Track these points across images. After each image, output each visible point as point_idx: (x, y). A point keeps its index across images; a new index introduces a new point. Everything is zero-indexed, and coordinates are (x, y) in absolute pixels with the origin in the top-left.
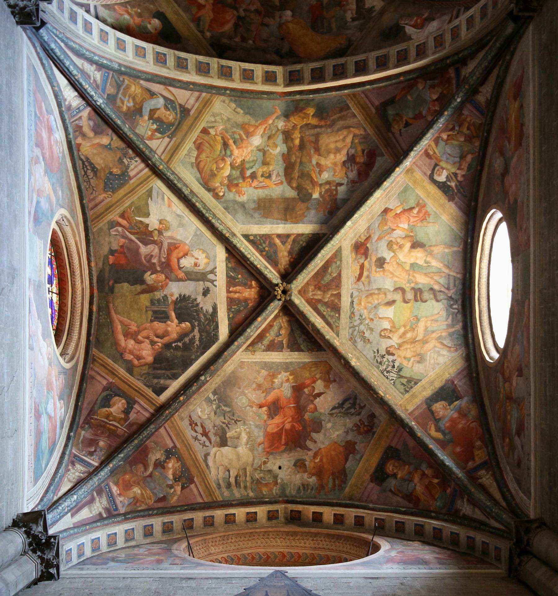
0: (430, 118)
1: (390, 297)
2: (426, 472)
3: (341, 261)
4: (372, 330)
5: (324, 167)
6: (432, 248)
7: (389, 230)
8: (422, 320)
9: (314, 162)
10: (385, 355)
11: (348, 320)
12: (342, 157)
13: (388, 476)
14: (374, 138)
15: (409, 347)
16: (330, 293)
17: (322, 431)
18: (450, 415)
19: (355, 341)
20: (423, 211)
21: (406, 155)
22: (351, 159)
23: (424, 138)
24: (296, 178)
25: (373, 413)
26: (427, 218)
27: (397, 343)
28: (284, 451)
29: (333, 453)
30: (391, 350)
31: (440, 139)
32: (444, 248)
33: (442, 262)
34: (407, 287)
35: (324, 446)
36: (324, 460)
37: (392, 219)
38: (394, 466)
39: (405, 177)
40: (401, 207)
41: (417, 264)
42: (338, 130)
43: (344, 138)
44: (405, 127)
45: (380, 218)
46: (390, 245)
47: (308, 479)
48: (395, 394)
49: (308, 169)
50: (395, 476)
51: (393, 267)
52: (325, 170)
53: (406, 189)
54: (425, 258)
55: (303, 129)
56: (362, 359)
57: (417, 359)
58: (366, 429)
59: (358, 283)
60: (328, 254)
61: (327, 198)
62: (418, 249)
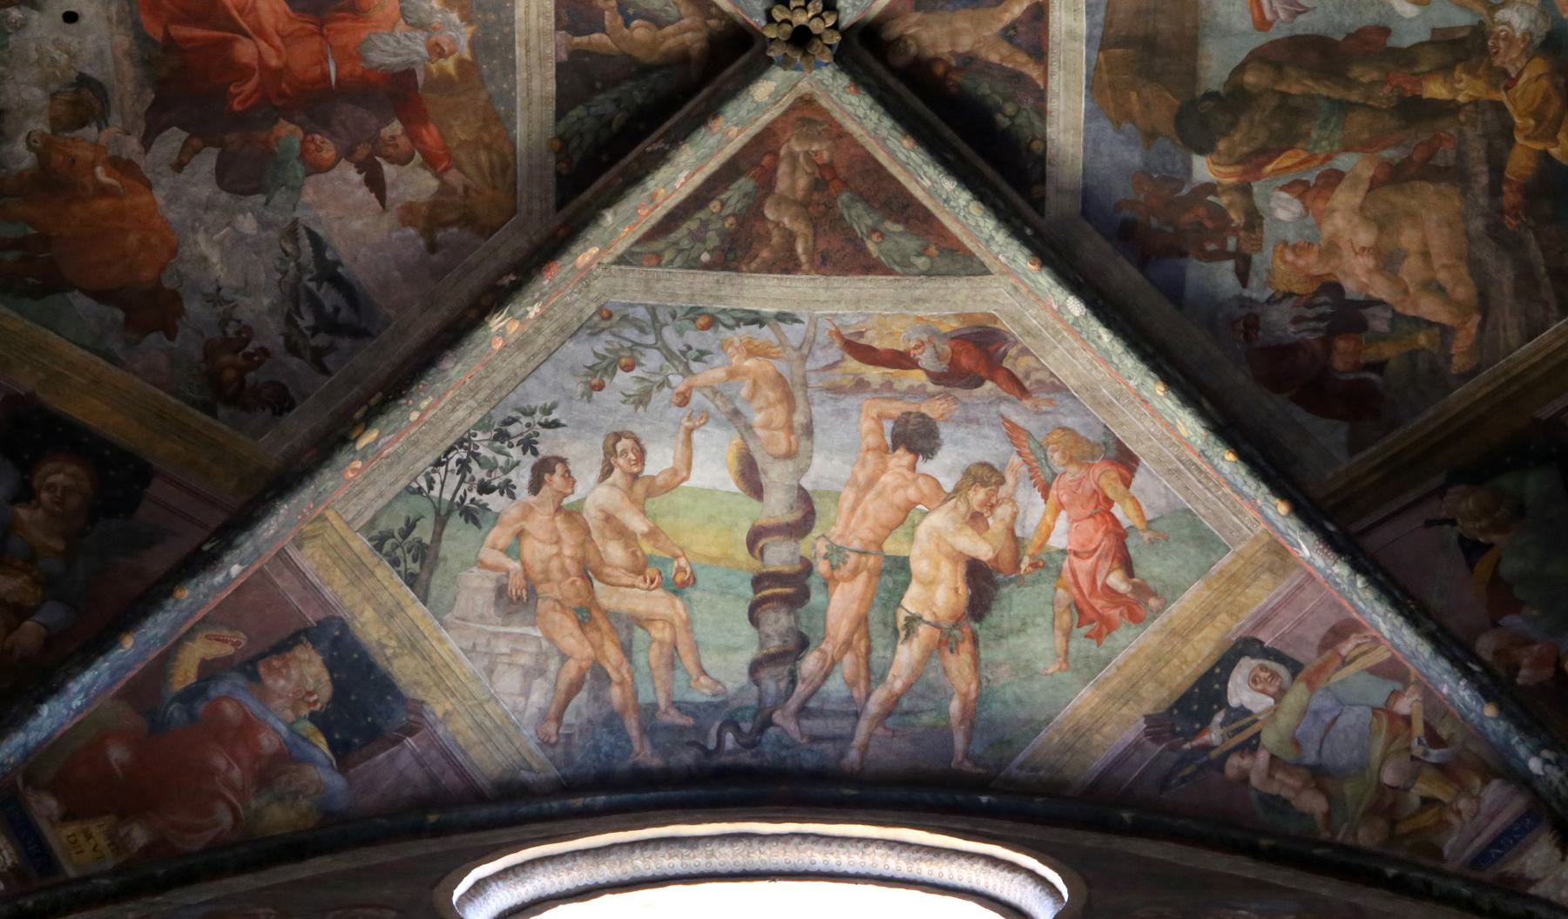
0: (1486, 645)
1: (775, 475)
2: (28, 623)
3: (929, 273)
4: (642, 399)
5: (1320, 204)
6: (966, 647)
7: (1045, 474)
8: (678, 603)
9: (1344, 162)
10: (535, 453)
11: (684, 302)
12: (1358, 276)
13: (26, 468)
14: (1431, 412)
15: (567, 551)
16: (799, 227)
17: (224, 197)
18: (271, 719)
19: (595, 333)
20: (1115, 613)
21: (1342, 544)
22: (1345, 314)
23: (1399, 621)
24: (1283, 87)
25: (290, 409)
26: (1086, 629)
27: (582, 501)
28: (141, 37)
29: (133, 239)
30: (557, 479)
31: (1398, 686)
32: (965, 695)
33: (908, 687)
34: (813, 546)
35: (160, 201)
36: (103, 205)
37: (1089, 485)
38: (65, 489)
39: (1257, 539)
40: (1137, 522)
41: (906, 585)
42: (1475, 266)
43: (1440, 289)
44: (1462, 540)
45: (1096, 436)
46: (984, 475)
47: (23, 136)
48: (370, 494)
49: (1314, 135)
50: (25, 494)
51: (897, 488)
52: (1306, 208)
53: (1206, 542)
54: (927, 617)
55: (1489, 116)
56: (520, 359)
57: (516, 585)
58: (230, 374)
59: (838, 344)
60: (957, 220)
61: (1187, 218)
62: (964, 592)
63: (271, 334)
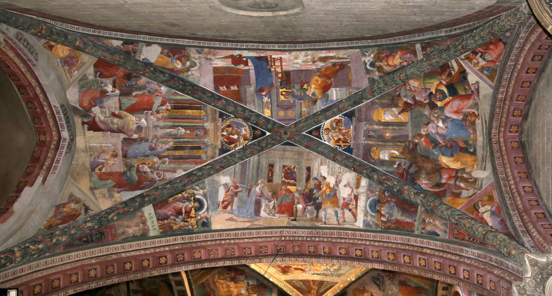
3: (293, 280)
11: (328, 277)
12: (232, 284)
16: (312, 286)
19: (340, 274)
22: (233, 279)
29: (406, 292)
42: (216, 286)
60: (289, 288)
63: (386, 279)
